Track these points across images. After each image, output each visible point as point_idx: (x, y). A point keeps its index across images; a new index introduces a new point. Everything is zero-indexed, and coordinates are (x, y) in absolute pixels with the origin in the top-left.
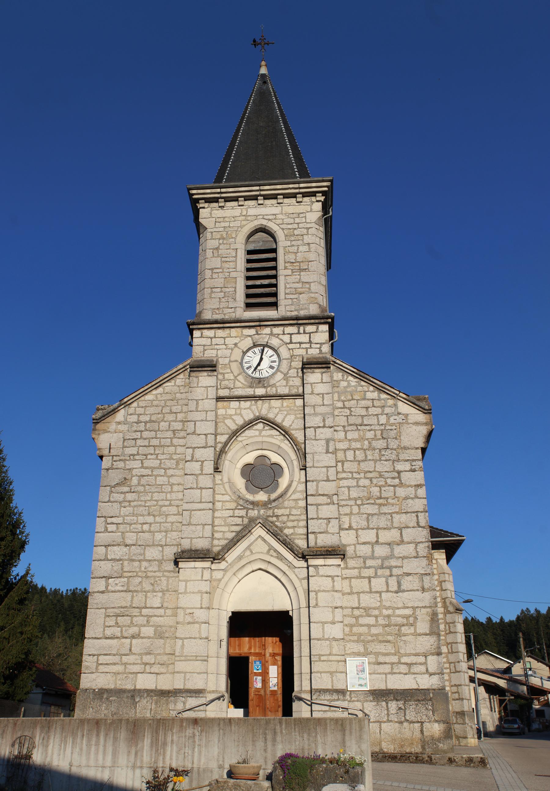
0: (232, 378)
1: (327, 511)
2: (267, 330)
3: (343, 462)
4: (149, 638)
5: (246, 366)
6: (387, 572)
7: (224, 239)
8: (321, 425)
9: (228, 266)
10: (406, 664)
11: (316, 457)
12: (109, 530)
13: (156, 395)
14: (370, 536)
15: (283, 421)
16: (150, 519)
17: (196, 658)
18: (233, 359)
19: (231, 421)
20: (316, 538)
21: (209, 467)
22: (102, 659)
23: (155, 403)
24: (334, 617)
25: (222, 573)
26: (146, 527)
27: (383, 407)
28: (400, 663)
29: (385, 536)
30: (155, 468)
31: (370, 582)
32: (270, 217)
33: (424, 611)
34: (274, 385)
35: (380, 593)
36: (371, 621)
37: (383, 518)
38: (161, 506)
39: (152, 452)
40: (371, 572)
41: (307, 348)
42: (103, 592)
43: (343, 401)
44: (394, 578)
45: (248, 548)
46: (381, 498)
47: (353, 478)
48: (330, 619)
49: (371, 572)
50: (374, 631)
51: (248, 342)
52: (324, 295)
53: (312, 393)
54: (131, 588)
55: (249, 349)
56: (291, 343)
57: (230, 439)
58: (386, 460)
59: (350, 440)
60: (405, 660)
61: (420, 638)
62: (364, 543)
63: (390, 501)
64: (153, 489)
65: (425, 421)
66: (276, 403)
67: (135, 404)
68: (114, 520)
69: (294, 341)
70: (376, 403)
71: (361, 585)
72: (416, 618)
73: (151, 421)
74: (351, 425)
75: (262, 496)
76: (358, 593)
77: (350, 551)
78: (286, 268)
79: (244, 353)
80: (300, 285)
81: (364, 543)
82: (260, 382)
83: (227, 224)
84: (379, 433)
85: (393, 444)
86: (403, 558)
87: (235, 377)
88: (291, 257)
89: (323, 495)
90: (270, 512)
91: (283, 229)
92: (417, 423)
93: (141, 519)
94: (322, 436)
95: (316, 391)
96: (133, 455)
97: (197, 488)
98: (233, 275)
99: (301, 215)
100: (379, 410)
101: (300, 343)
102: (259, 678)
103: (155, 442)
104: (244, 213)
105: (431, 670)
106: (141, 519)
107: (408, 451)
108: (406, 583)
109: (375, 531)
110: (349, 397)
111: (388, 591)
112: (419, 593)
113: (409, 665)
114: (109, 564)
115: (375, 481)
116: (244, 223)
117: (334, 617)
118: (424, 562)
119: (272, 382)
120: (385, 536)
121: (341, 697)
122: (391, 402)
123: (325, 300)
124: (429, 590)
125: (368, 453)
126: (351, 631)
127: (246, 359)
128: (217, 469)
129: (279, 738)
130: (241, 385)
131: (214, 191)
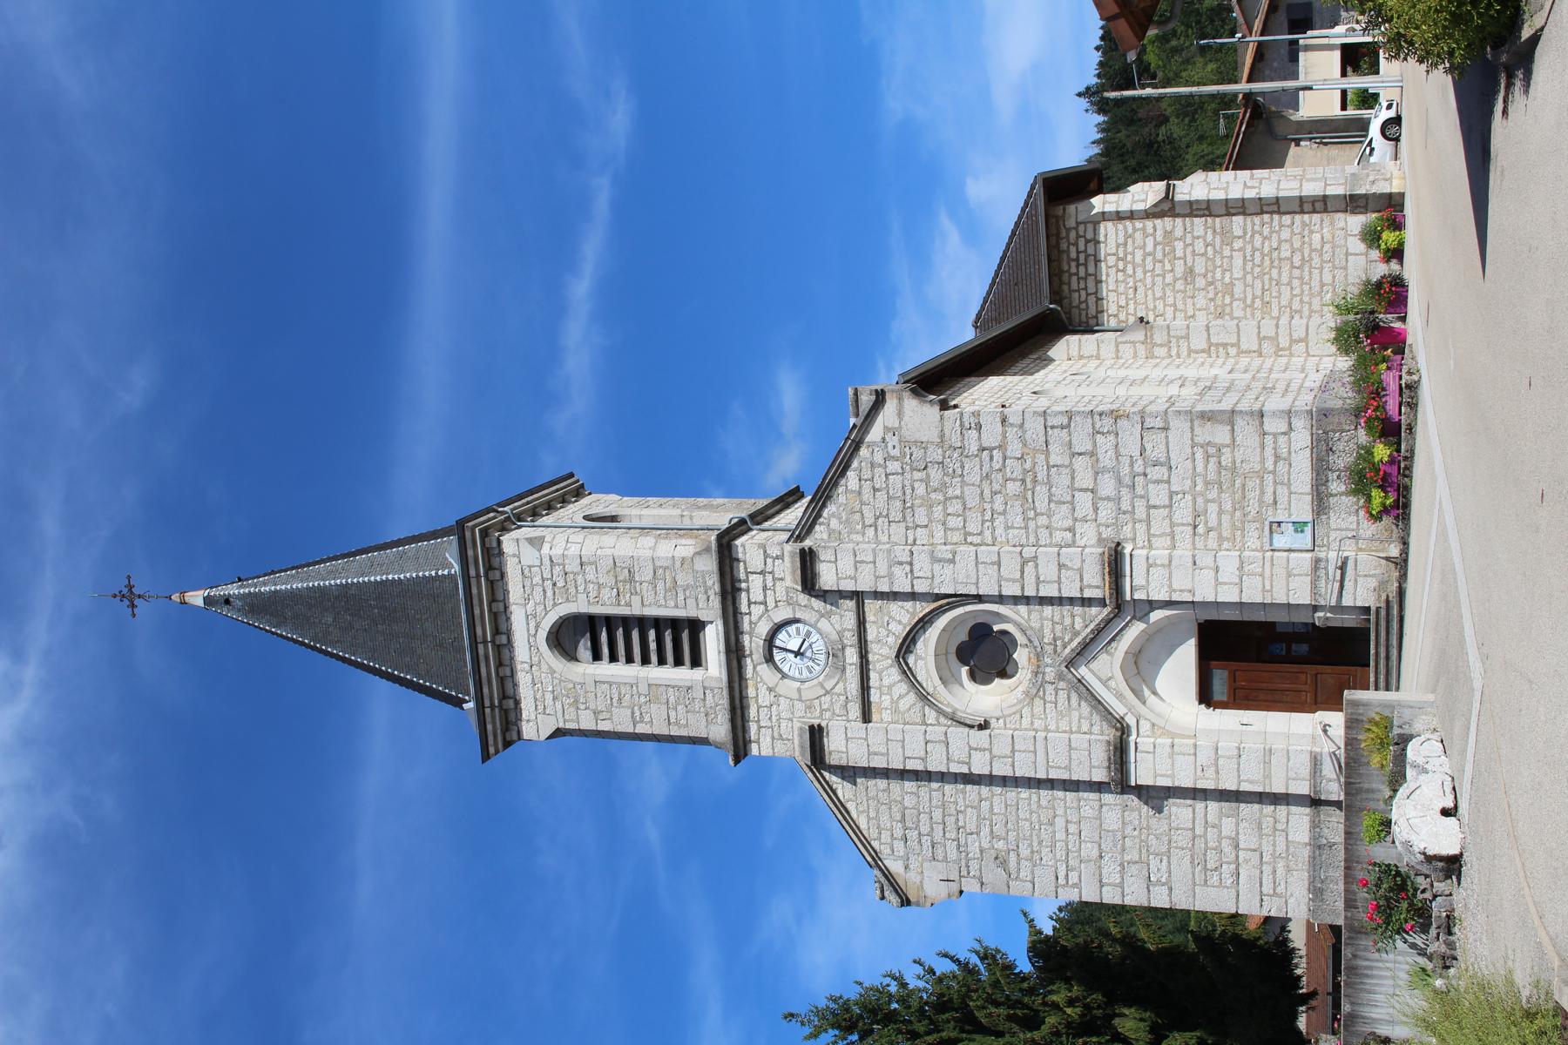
0: (828, 698)
1: (1048, 570)
2: (746, 639)
3: (967, 534)
4: (1237, 824)
5: (806, 674)
6: (1140, 480)
7: (576, 701)
8: (908, 568)
9: (628, 697)
10: (1275, 463)
11: (961, 578)
12: (1076, 880)
13: (860, 813)
14: (1084, 502)
15: (900, 622)
16: (1060, 822)
17: (1267, 763)
18: (795, 695)
19: (902, 702)
20: (1090, 586)
21: (980, 737)
22: (1267, 888)
23: (872, 814)
24: (1207, 568)
25: (1142, 722)
26: (1073, 828)
27: (872, 465)
28: (1274, 472)
29: (1085, 479)
30: (979, 816)
31: (1154, 507)
32: (532, 624)
33: (1198, 430)
34: (840, 634)
35: (1171, 494)
36: (1213, 508)
37: (1055, 479)
38: (1039, 806)
39: (953, 819)
40: (1140, 507)
41: (774, 579)
42: (1171, 889)
43: (864, 526)
44: (1148, 470)
45: (1104, 683)
46: (1023, 481)
47: (992, 520)
48: (1212, 573)
49: (1140, 507)
50: (1228, 506)
51: (764, 669)
52: (674, 542)
53: (855, 578)
54: (1164, 849)
55: (777, 668)
56: (765, 603)
57: (932, 705)
58: (963, 467)
59: (930, 521)
60: (1269, 465)
61: (1238, 439)
62: (1096, 510)
63: (1028, 465)
64: (1012, 818)
65: (895, 401)
66: (872, 633)
67: (875, 844)
68: (1061, 875)
69: (761, 598)
70: (866, 474)
71: (1159, 523)
72: (1209, 443)
73: (903, 820)
74: (904, 517)
75: (1021, 656)
76: (1172, 525)
77: (1107, 533)
78: (629, 605)
79: (784, 676)
80: (660, 585)
81: (1096, 510)
82: (835, 654)
83: (549, 697)
84: (917, 475)
85: (936, 454)
86: (1118, 455)
87: (827, 692)
88: (608, 594)
89: (1022, 572)
90: (1049, 649)
91: (555, 605)
92: (900, 414)
93: (1060, 835)
94: (927, 567)
95: (851, 572)
96: (959, 846)
97: (1013, 757)
98: (643, 689)
99: (526, 572)
100: (878, 471)
101: (765, 588)
102: (1294, 647)
103: (937, 815)
104: (527, 667)
105: (1284, 428)
106: (1060, 835)
107: (947, 432)
108: (1156, 453)
109: (1077, 494)
110: (857, 516)
111: (1168, 482)
112: (1171, 434)
113: (1277, 457)
114: (1128, 880)
115: (996, 487)
116: (544, 667)
117: (1207, 568)
118: (1123, 423)
119: (834, 637)
120: (1085, 479)
121: (1322, 565)
122: (863, 452)
123: (683, 541)
124: (1166, 421)
125: (950, 492)
126: (1228, 539)
127: (794, 673)
128: (984, 726)
129: (1366, 786)
130: (841, 685)
131: (488, 719)
